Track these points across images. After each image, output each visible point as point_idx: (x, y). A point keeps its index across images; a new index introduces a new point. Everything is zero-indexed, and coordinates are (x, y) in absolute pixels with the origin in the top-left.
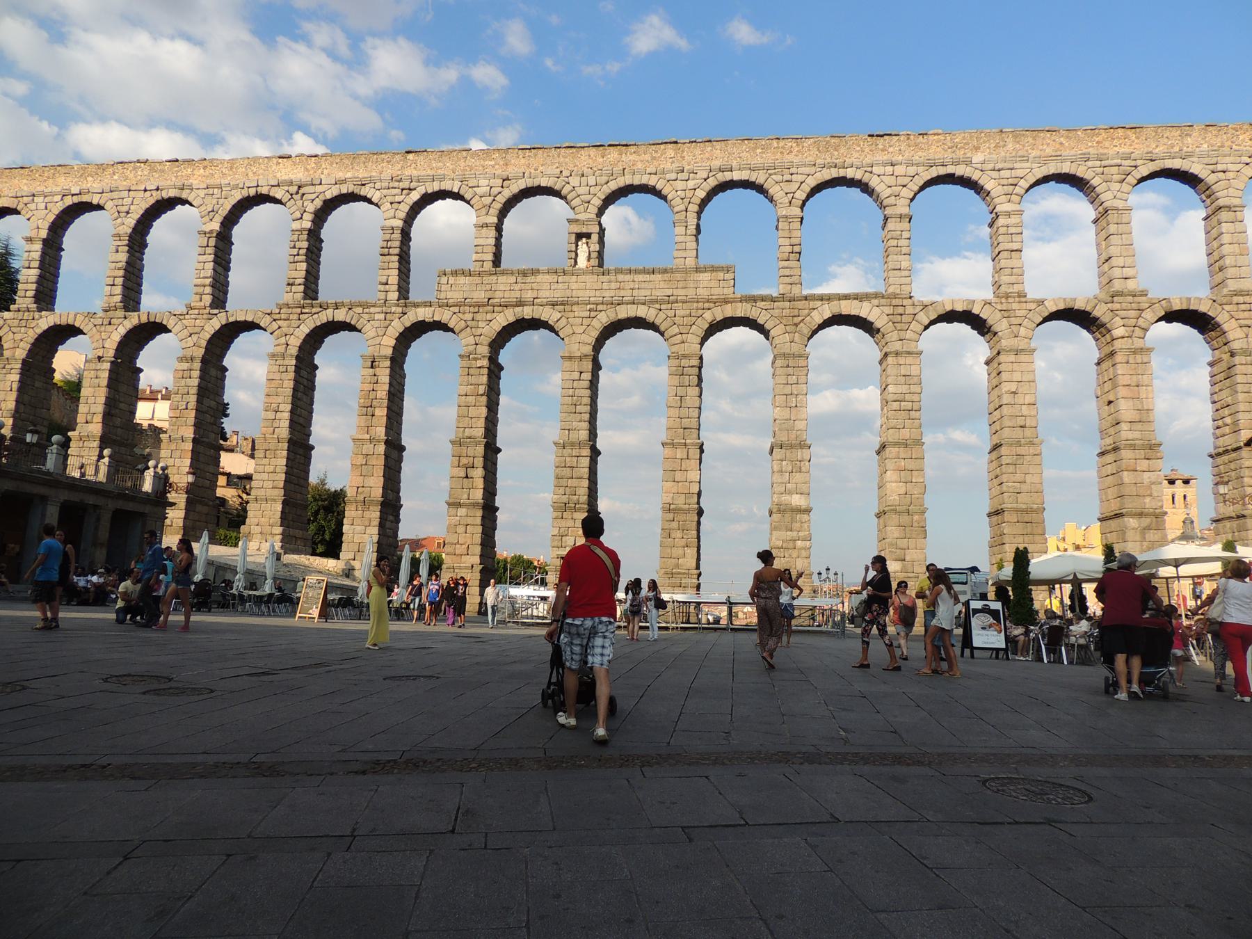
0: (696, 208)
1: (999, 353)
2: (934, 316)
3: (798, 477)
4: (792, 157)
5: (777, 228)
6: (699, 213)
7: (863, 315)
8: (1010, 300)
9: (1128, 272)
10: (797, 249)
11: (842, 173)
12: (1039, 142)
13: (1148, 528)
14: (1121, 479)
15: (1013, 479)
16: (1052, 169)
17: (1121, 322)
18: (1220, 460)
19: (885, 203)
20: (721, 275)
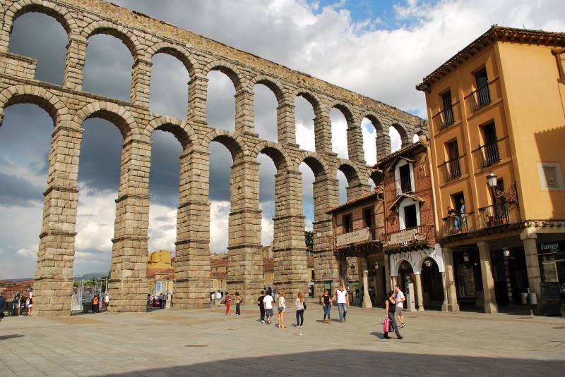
0: (12, 14)
1: (192, 152)
2: (160, 124)
3: (69, 211)
4: (85, 6)
5: (67, 47)
6: (14, 19)
7: (120, 113)
8: (200, 125)
9: (251, 124)
10: (82, 62)
11: (115, 26)
12: (218, 48)
13: (255, 253)
14: (245, 227)
15: (196, 223)
16: (223, 63)
17: (248, 148)
18: (279, 222)
19: (139, 52)
20: (26, 64)
